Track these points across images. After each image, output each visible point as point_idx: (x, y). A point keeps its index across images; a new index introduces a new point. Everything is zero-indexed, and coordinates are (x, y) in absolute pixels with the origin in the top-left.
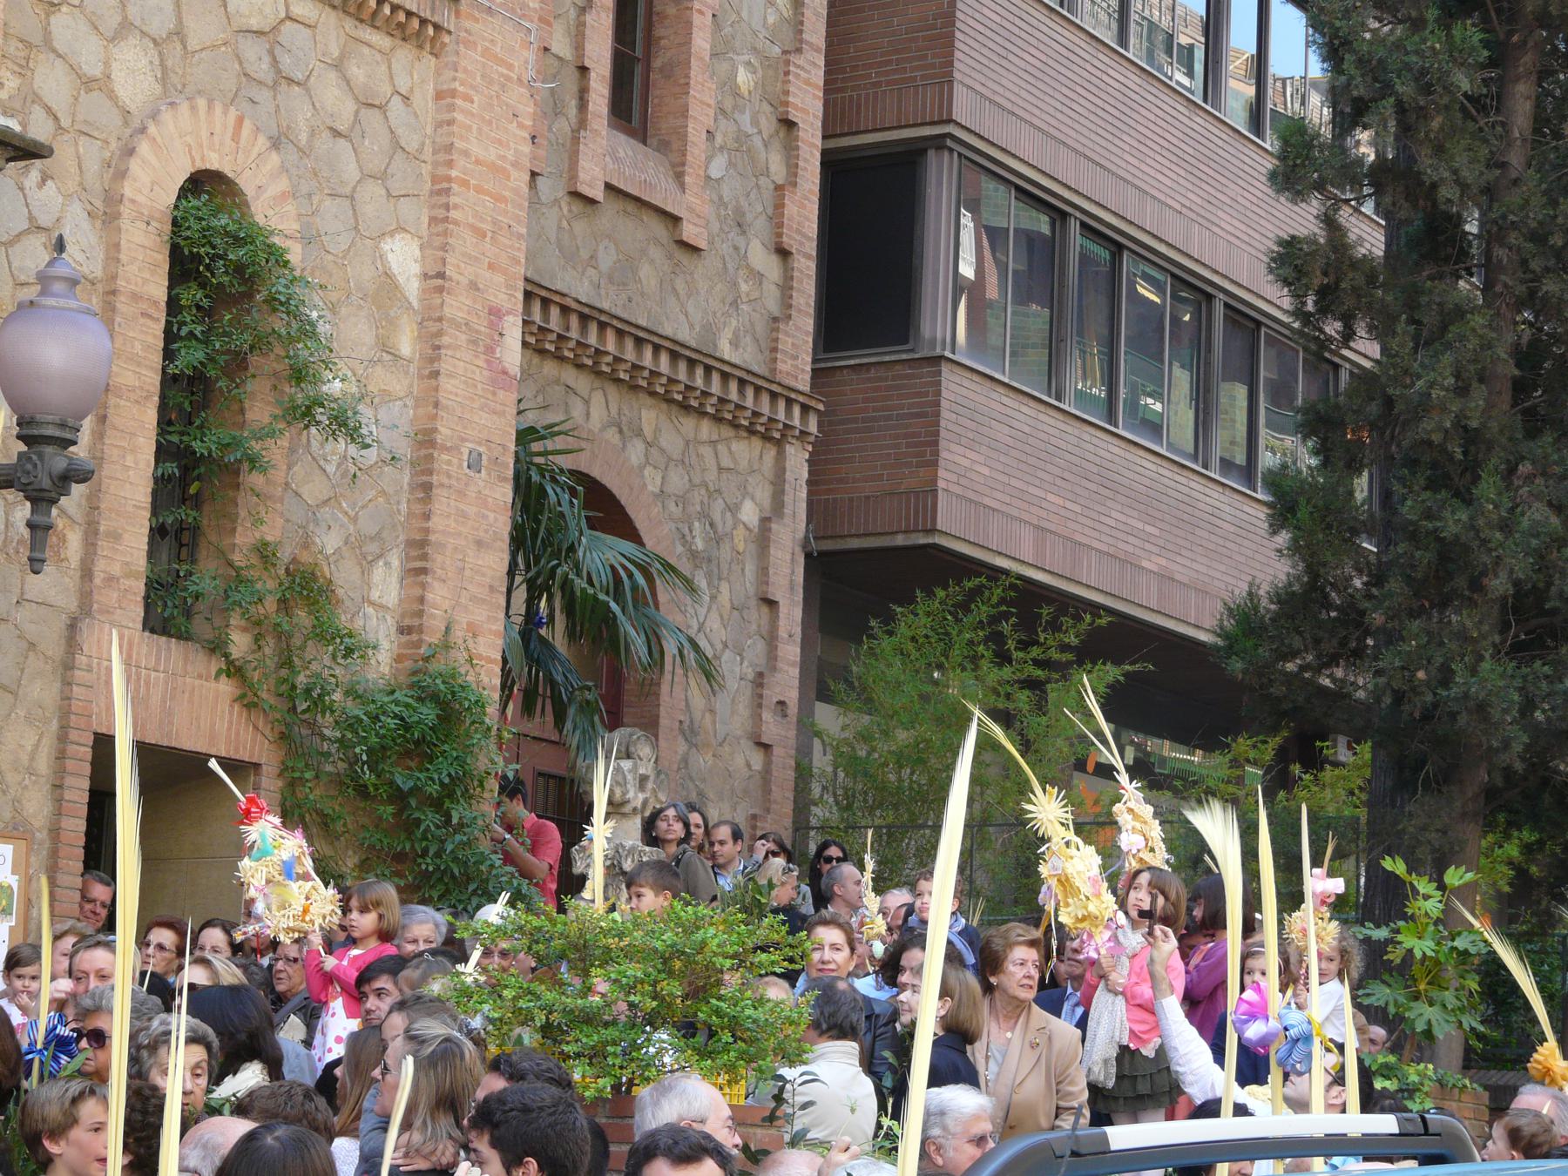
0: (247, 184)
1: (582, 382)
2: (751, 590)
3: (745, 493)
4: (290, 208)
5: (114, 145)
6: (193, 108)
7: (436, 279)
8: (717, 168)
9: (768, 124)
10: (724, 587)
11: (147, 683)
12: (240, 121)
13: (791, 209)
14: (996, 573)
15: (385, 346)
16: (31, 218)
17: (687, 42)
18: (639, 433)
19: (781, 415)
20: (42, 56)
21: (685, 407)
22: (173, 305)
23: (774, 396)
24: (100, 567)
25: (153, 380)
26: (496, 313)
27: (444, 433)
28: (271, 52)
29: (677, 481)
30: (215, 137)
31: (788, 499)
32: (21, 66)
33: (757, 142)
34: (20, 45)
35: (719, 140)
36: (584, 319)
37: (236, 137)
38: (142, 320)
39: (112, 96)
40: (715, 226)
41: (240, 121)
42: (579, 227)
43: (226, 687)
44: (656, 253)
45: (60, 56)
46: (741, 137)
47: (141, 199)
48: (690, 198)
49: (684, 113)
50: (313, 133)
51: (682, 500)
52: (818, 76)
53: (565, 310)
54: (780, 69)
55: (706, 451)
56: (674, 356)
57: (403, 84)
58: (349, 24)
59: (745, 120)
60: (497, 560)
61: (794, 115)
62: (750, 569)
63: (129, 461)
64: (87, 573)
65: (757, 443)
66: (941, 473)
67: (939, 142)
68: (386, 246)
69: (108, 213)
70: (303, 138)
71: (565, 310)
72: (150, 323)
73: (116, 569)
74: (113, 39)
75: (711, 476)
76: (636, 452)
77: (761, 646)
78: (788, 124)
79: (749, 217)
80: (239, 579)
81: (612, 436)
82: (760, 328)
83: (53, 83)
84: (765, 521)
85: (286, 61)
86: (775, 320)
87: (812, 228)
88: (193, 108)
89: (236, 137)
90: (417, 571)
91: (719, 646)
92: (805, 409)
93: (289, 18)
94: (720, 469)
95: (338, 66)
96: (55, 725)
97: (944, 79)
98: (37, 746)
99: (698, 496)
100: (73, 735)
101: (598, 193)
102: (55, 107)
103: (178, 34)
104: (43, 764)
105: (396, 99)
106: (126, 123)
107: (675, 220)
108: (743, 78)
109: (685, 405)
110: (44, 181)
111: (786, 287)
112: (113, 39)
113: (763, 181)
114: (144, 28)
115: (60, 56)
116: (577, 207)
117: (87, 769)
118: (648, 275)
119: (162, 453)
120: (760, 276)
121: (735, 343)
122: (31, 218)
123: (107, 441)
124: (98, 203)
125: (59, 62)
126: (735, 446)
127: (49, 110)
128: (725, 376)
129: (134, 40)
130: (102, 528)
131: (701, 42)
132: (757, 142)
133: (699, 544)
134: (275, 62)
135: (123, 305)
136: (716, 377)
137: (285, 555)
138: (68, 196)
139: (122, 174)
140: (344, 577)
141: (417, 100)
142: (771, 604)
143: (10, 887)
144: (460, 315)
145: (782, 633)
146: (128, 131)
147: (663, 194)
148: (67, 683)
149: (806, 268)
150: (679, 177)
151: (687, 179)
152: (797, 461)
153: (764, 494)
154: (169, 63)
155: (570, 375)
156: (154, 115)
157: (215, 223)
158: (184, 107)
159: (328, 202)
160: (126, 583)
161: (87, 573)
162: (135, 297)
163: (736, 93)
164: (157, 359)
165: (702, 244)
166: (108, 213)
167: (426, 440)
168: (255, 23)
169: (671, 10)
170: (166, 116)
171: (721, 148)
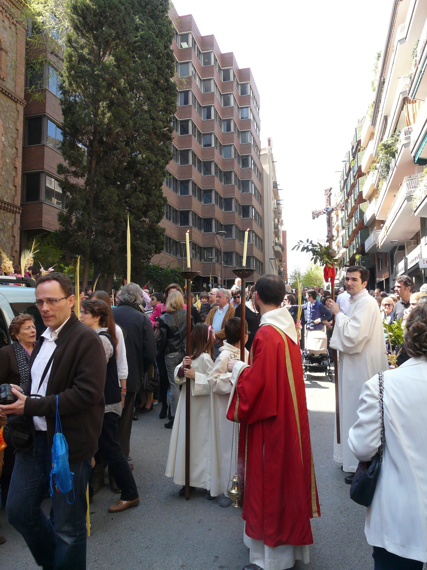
2: (11, 234)
3: (9, 220)
9: (12, 167)
10: (6, 234)
13: (16, 180)
19: (15, 209)
23: (14, 207)
31: (17, 221)
33: (10, 170)
35: (3, 169)
40: (3, 182)
46: (7, 169)
52: (21, 161)
54: (14, 160)
55: (2, 214)
59: (8, 167)
61: (16, 166)
62: (10, 231)
65: (11, 213)
66: (43, 219)
67: (42, 172)
75: (3, 218)
79: (9, 181)
84: (13, 225)
86: (14, 196)
87: (20, 183)
91: (5, 242)
92: (19, 209)
94: (5, 217)
97: (43, 163)
108: (7, 160)
111: (16, 191)
113: (12, 176)
120: (11, 189)
121: (7, 199)
126: (7, 214)
128: (5, 204)
132: (10, 170)
136: (3, 204)
142: (14, 237)
145: (16, 241)
149: (19, 189)
152: (18, 216)
153: (13, 221)
163: (6, 162)
171: (4, 171)
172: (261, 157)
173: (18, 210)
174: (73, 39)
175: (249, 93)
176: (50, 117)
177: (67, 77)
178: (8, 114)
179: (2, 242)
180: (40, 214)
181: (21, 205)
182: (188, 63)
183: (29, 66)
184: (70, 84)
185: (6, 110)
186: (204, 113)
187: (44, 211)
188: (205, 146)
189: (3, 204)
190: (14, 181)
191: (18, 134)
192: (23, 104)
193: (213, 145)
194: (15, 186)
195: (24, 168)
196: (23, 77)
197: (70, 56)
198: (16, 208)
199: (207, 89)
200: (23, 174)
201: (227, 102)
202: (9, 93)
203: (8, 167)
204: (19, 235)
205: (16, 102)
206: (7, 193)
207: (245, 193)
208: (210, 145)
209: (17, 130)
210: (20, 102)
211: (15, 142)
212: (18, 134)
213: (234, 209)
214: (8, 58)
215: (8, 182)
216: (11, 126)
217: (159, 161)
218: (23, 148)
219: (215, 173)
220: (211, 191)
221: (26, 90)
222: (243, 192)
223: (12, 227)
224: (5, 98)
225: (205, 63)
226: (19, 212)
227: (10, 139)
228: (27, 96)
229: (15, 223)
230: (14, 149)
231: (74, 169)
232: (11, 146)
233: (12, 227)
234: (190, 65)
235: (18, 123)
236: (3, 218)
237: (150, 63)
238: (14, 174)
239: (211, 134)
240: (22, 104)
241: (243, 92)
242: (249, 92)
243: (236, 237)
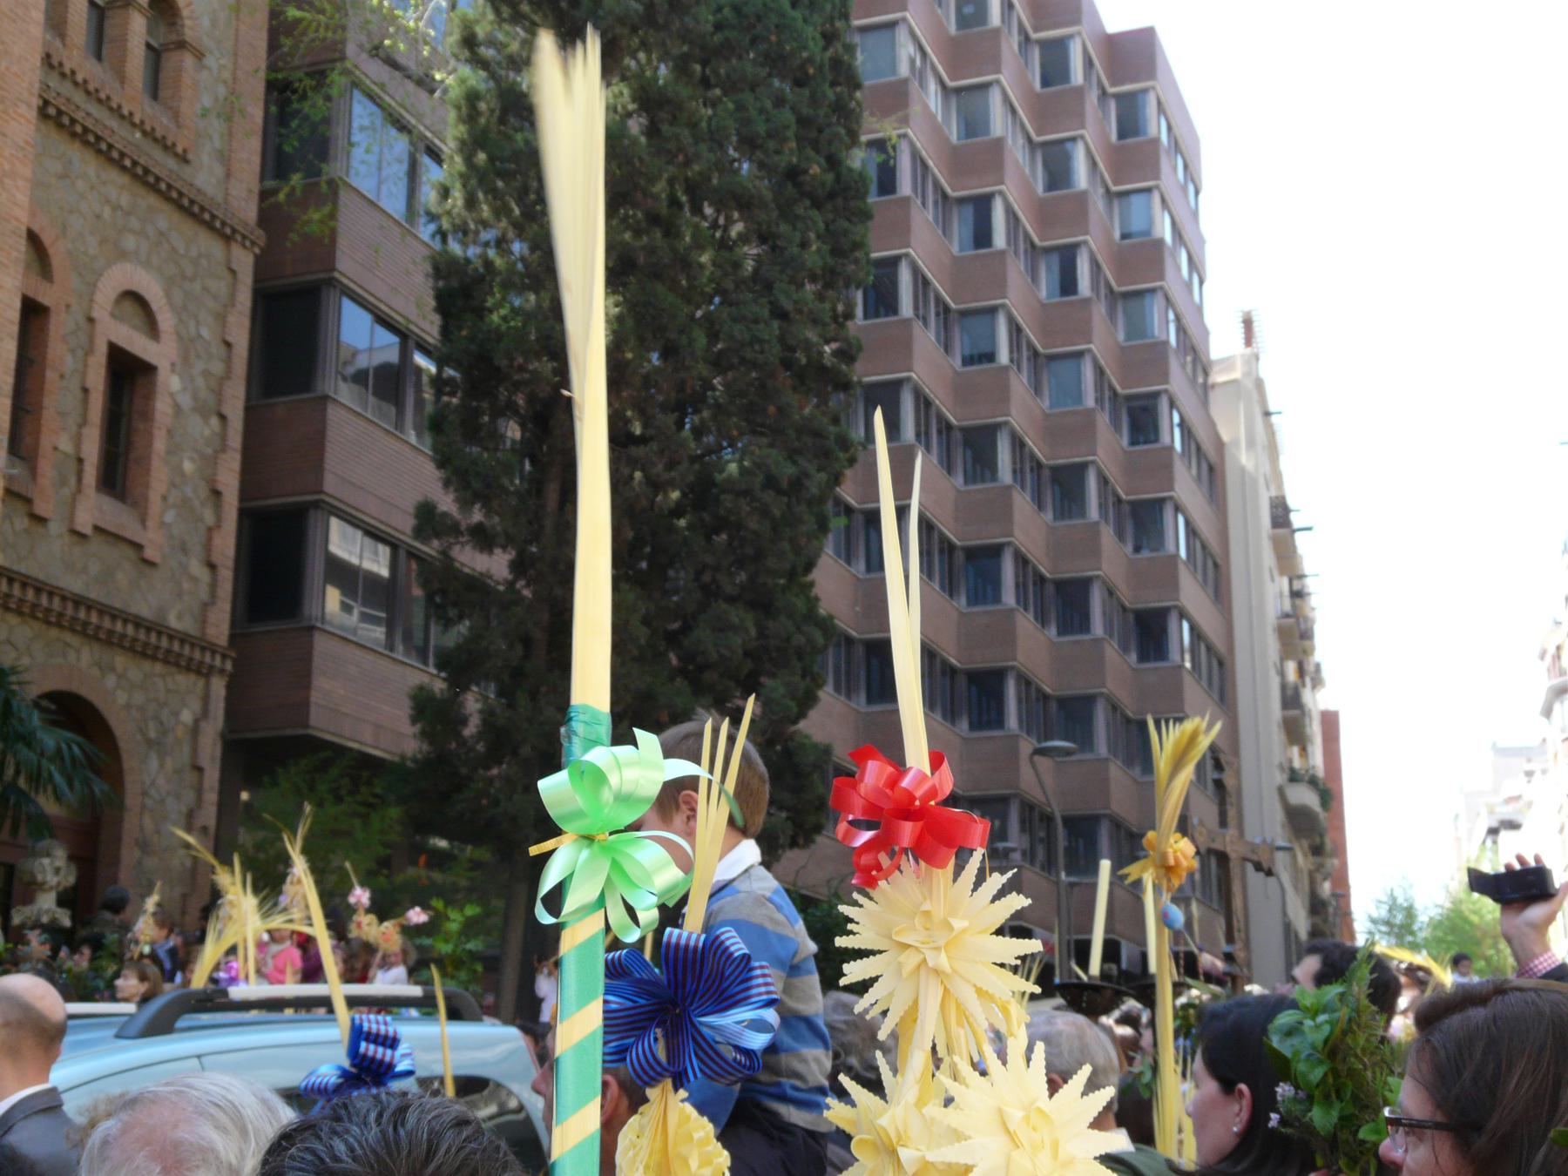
8: (169, 517)
9: (204, 492)
13: (217, 541)
14: (340, 750)
17: (149, 445)
18: (113, 669)
19: (208, 659)
21: (144, 655)
29: (139, 698)
31: (212, 707)
35: (171, 500)
49: (147, 486)
53: (64, 598)
54: (210, 463)
61: (220, 488)
62: (186, 749)
66: (313, 693)
71: (64, 598)
76: (111, 681)
78: (217, 494)
81: (95, 671)
84: (197, 721)
87: (230, 551)
92: (224, 657)
97: (318, 466)
101: (88, 530)
108: (188, 466)
109: (144, 653)
111: (213, 585)
116: (75, 538)
118: (121, 578)
121: (180, 617)
131: (160, 444)
133: (152, 734)
142: (200, 770)
147: (132, 530)
149: (226, 575)
150: (143, 522)
151: (148, 523)
152: (219, 687)
153: (195, 705)
155: (68, 637)
163: (183, 474)
165: (158, 560)
169: (141, 426)
172: (1214, 396)
173: (218, 662)
174: (481, 31)
175: (1152, 130)
176: (352, 285)
177: (461, 175)
178: (197, 287)
179: (153, 792)
180: (303, 678)
181: (234, 638)
182: (892, 25)
183: (280, 92)
184: (471, 203)
185: (189, 271)
186: (961, 225)
187: (317, 661)
188: (968, 360)
190: (208, 546)
191: (228, 362)
192: (253, 243)
193: (1003, 357)
195: (244, 494)
196: (255, 144)
197: (472, 97)
199: (973, 125)
200: (243, 513)
201: (1058, 174)
202: (203, 209)
203: (189, 491)
204: (218, 764)
205: (228, 239)
206: (180, 595)
207: (1145, 554)
208: (990, 357)
209: (228, 345)
210: (244, 237)
211: (218, 393)
212: (228, 362)
213: (1098, 627)
214: (205, 74)
216: (205, 333)
217: (807, 476)
218: (250, 410)
219: (1014, 472)
220: (995, 551)
221: (264, 195)
222: (1137, 549)
223: (195, 731)
224: (188, 227)
225: (963, 22)
226: (222, 671)
227: (200, 382)
228: (270, 216)
229: (206, 712)
230: (214, 422)
231: (477, 516)
232: (201, 410)
233: (195, 731)
234: (902, 35)
235: (232, 319)
237: (768, 104)
238: (209, 517)
239: (993, 311)
240: (248, 243)
241: (1130, 124)
242: (1157, 128)
243: (1113, 750)
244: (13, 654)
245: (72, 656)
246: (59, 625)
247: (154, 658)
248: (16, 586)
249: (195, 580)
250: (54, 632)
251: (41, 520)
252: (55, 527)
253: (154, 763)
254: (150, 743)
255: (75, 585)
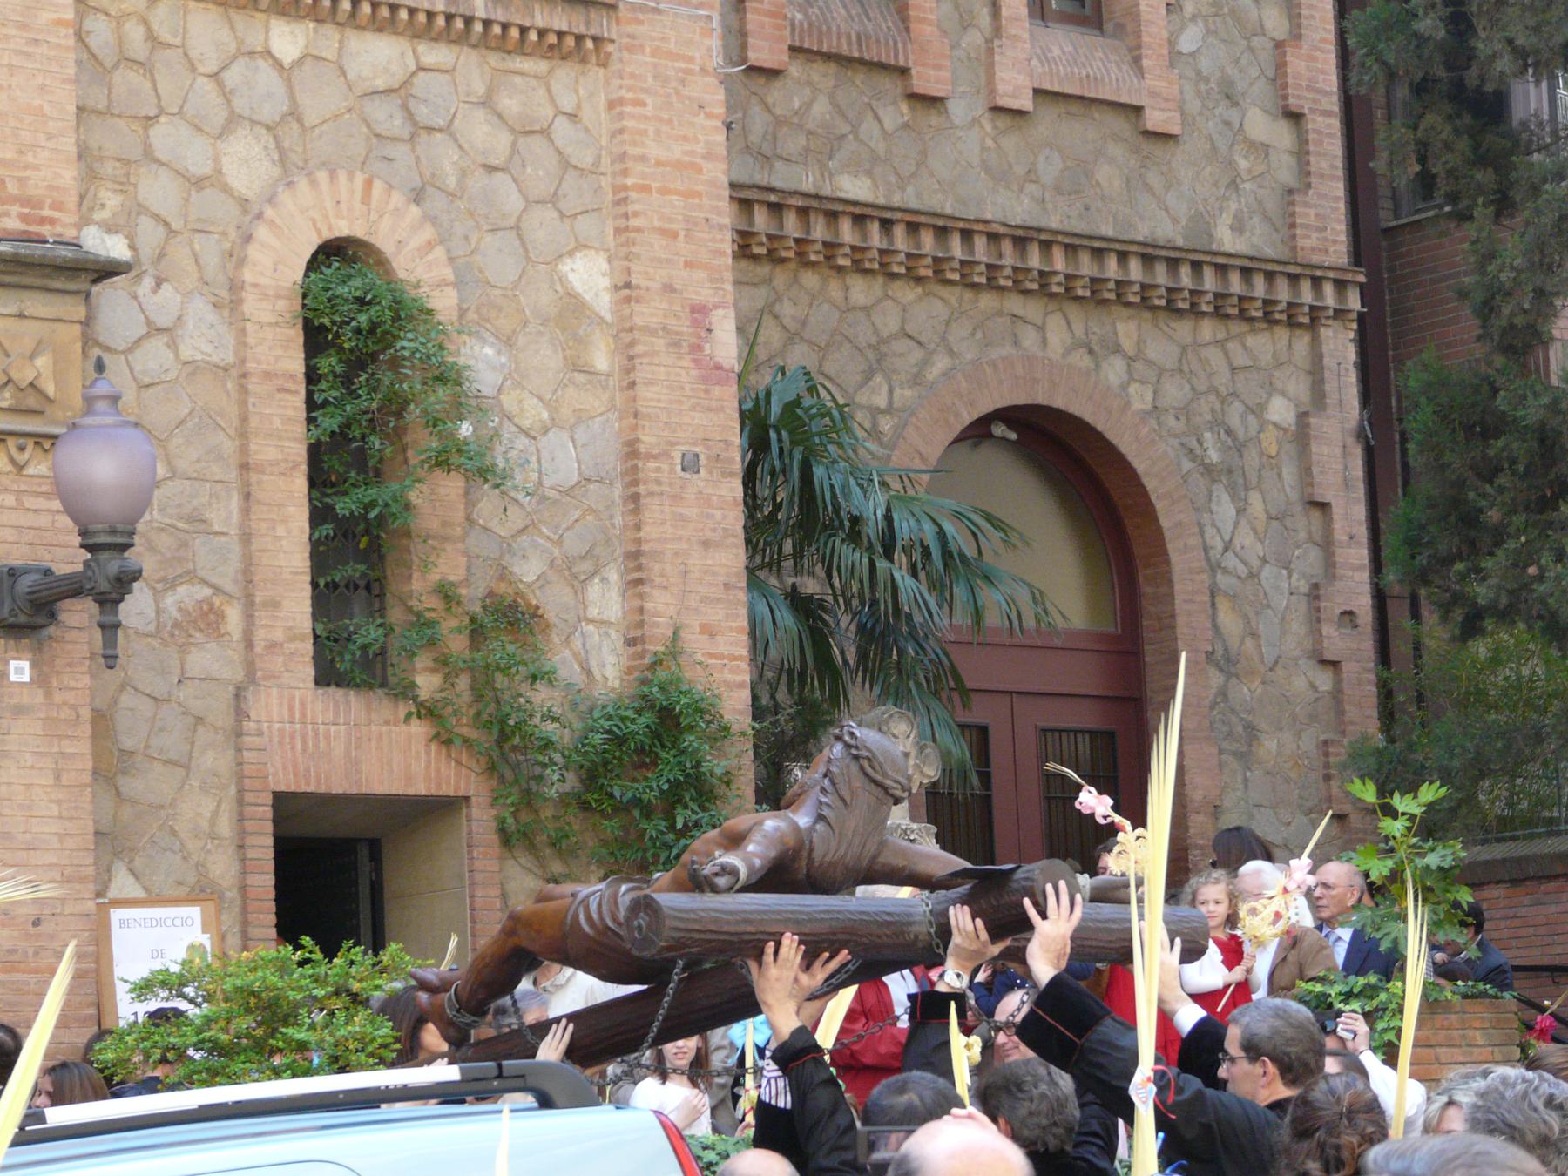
0: (384, 241)
1: (1032, 309)
2: (1294, 495)
3: (1271, 389)
4: (439, 253)
5: (233, 234)
6: (314, 183)
7: (625, 289)
8: (1189, 41)
10: (1255, 499)
11: (327, 737)
12: (369, 184)
13: (1297, 65)
15: (577, 366)
16: (149, 322)
18: (1117, 349)
20: (143, 170)
21: (1171, 309)
22: (312, 377)
23: (1294, 279)
24: (260, 635)
25: (299, 452)
26: (700, 312)
27: (648, 439)
28: (405, 107)
29: (1175, 392)
30: (343, 206)
32: (122, 183)
34: (118, 164)
36: (1020, 242)
37: (366, 198)
38: (279, 396)
39: (226, 189)
40: (1194, 106)
41: (369, 184)
42: (1010, 143)
43: (419, 729)
44: (1117, 151)
45: (163, 164)
47: (263, 281)
48: (1151, 81)
50: (463, 174)
51: (1185, 412)
53: (993, 237)
55: (1214, 356)
56: (1148, 260)
57: (567, 102)
58: (494, 59)
60: (732, 558)
62: (1289, 473)
63: (281, 530)
64: (249, 645)
65: (1282, 334)
68: (565, 267)
69: (230, 301)
70: (452, 182)
71: (993, 237)
72: (288, 396)
73: (278, 635)
74: (221, 135)
75: (1222, 380)
76: (1114, 371)
77: (1314, 555)
79: (1240, 86)
80: (422, 623)
81: (1081, 360)
82: (1272, 205)
83: (158, 191)
84: (1302, 417)
85: (423, 113)
86: (1291, 192)
88: (314, 183)
89: (366, 198)
90: (636, 584)
91: (1255, 563)
92: (1340, 285)
93: (421, 68)
94: (1233, 369)
95: (487, 102)
96: (233, 790)
98: (216, 813)
99: (1205, 407)
100: (249, 797)
101: (1026, 102)
102: (163, 214)
103: (292, 114)
104: (225, 827)
105: (561, 121)
106: (245, 212)
107: (1138, 110)
109: (1174, 307)
110: (158, 285)
111: (1302, 153)
112: (221, 135)
113: (1256, 41)
114: (255, 117)
115: (163, 164)
116: (1003, 122)
117: (269, 827)
118: (1108, 176)
119: (319, 515)
120: (1266, 147)
121: (1238, 227)
122: (149, 322)
123: (253, 517)
124: (224, 293)
125: (162, 171)
126: (1251, 341)
127: (157, 217)
128: (1222, 269)
129: (243, 132)
130: (258, 600)
133: (1214, 456)
134: (409, 115)
135: (254, 385)
136: (1208, 273)
137: (473, 595)
138: (187, 294)
139: (242, 262)
140: (553, 601)
141: (586, 114)
142: (1323, 506)
143: (202, 946)
144: (654, 321)
145: (1340, 535)
146: (248, 218)
147: (1115, 82)
148: (239, 750)
150: (1137, 60)
151: (1145, 63)
152: (1340, 346)
153: (1299, 387)
154: (286, 144)
155: (1015, 304)
156: (271, 200)
157: (343, 290)
158: (302, 184)
159: (489, 238)
160: (293, 646)
161: (249, 645)
162: (268, 375)
164: (300, 429)
165: (1175, 129)
166: (230, 301)
167: (632, 451)
168: (380, 83)
170: (284, 196)
171: (1194, 18)
173: (1329, 296)
179: (1231, 561)
189: (1208, 273)
190: (1279, 77)
194: (1294, 117)
198: (1317, 282)
204: (1360, 491)
206: (1233, 185)
215: (1231, 98)
223: (1302, 435)
226: (1339, 314)
233: (1302, 435)
236: (1222, 380)
244: (918, 354)
245: (1029, 338)
246: (992, 285)
247: (1195, 312)
248: (899, 232)
249: (1262, 149)
250: (987, 301)
251: (933, 102)
252: (958, 109)
253: (1225, 509)
254: (1209, 470)
255: (1016, 208)
